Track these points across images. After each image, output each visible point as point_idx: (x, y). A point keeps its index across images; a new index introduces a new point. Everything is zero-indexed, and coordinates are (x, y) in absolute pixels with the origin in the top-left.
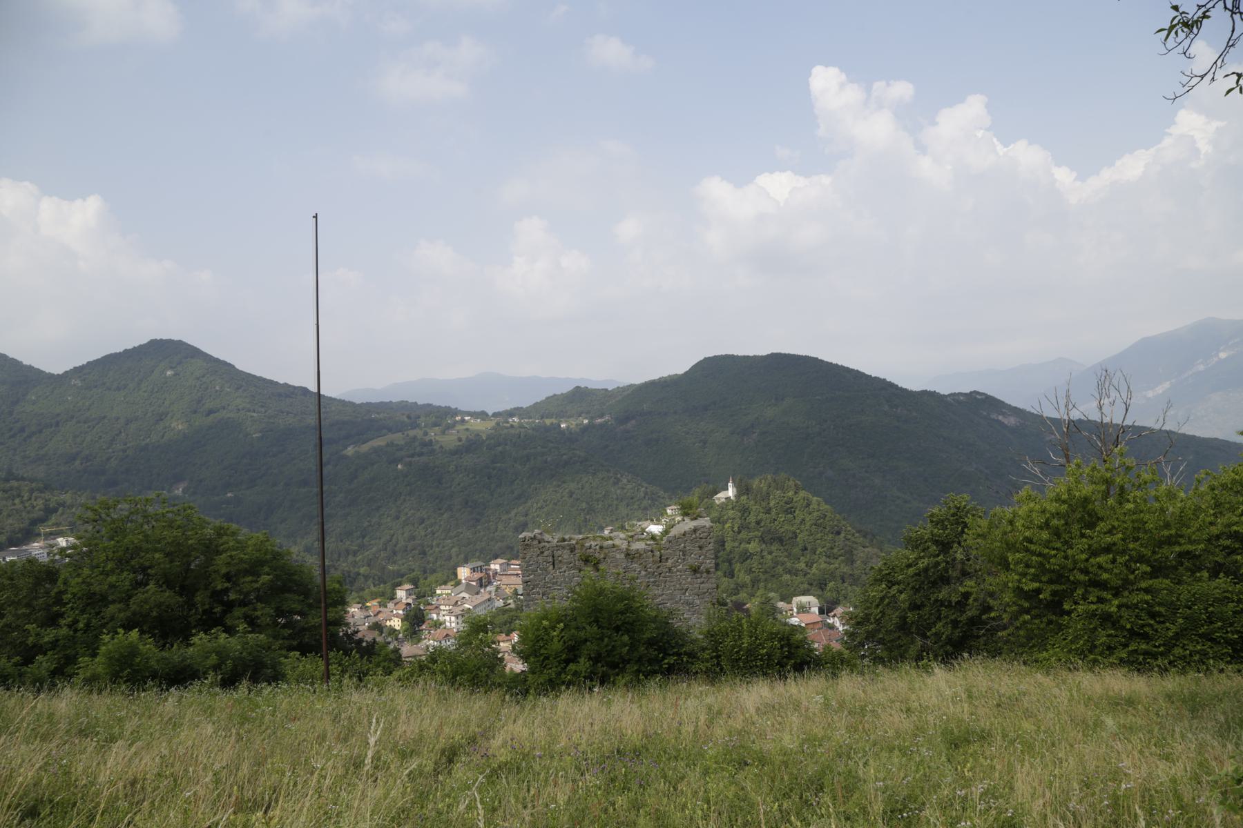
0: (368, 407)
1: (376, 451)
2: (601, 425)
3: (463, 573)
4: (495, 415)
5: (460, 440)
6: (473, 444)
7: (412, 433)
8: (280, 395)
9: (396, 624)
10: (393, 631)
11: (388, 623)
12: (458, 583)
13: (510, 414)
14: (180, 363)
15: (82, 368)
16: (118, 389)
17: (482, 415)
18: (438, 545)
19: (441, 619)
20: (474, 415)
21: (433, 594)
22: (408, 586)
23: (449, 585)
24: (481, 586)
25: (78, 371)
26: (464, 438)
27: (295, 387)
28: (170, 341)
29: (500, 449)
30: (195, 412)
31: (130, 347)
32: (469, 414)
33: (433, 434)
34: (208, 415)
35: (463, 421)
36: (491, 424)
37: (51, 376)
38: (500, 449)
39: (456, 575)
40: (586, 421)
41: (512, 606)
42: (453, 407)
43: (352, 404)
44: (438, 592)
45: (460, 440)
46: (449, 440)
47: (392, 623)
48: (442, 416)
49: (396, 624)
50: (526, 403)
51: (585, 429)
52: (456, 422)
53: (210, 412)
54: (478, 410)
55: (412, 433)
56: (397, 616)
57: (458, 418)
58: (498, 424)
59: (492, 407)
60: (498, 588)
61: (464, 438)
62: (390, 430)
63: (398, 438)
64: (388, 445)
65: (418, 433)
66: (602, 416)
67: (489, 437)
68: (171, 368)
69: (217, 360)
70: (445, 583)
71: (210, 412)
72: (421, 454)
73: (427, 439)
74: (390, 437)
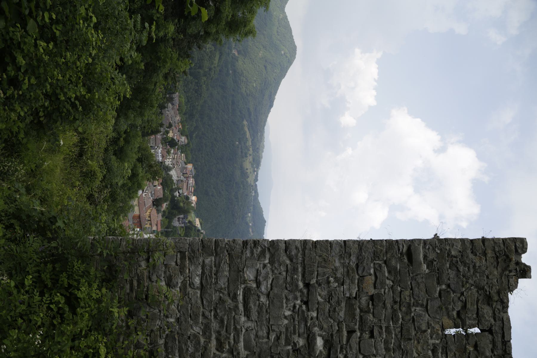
0: (262, 132)
1: (245, 134)
2: (249, 231)
3: (190, 166)
4: (256, 185)
5: (247, 169)
6: (244, 175)
7: (251, 149)
8: (271, 96)
9: (171, 135)
10: (167, 132)
11: (171, 131)
12: (186, 164)
13: (256, 192)
14: (287, 57)
15: (287, 19)
16: (277, 32)
17: (256, 180)
18: (202, 157)
19: (171, 155)
20: (257, 176)
21: (182, 152)
22: (186, 141)
23: (185, 160)
24: (184, 174)
25: (286, 17)
26: (247, 171)
27: (273, 102)
28: (295, 54)
29: (242, 186)
30: (266, 61)
31: (294, 38)
32: (257, 174)
33: (250, 158)
34: (264, 66)
35: (254, 171)
36: (252, 184)
37: (284, 7)
38: (242, 186)
39: (189, 163)
40: (251, 224)
41: (174, 187)
42: (260, 168)
43: (264, 125)
44: (183, 155)
45: (247, 169)
46: (247, 165)
47: (171, 133)
48: (257, 163)
49: (171, 135)
50: (260, 198)
51: (247, 224)
52: (254, 168)
53: (265, 67)
54: (259, 178)
55: (251, 149)
56: (174, 135)
57: (256, 169)
58: (252, 186)
59: (261, 186)
60: (182, 181)
61: (247, 171)
62: (253, 140)
63: (249, 143)
64: (247, 138)
65: (251, 152)
66: (252, 232)
67: (247, 182)
68: (285, 54)
69: (287, 72)
70: (186, 158)
71: (265, 67)
72: (242, 152)
73: (248, 155)
74: (250, 140)
